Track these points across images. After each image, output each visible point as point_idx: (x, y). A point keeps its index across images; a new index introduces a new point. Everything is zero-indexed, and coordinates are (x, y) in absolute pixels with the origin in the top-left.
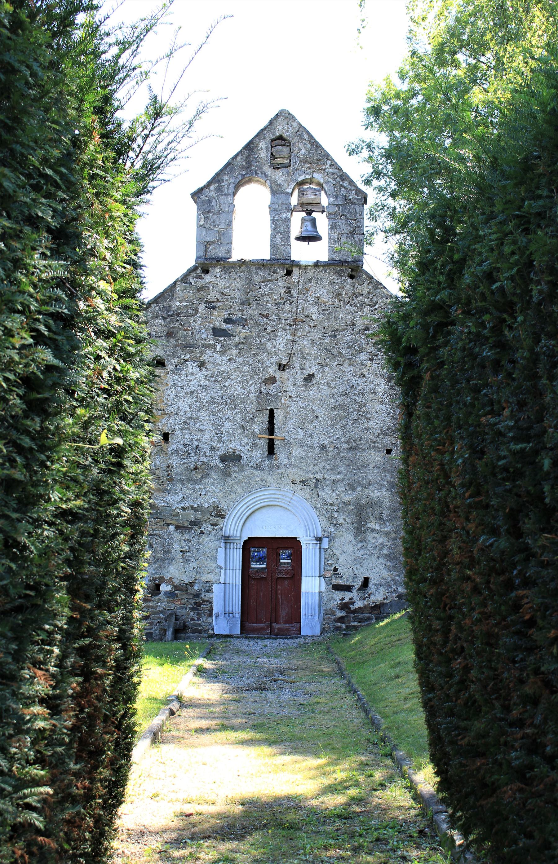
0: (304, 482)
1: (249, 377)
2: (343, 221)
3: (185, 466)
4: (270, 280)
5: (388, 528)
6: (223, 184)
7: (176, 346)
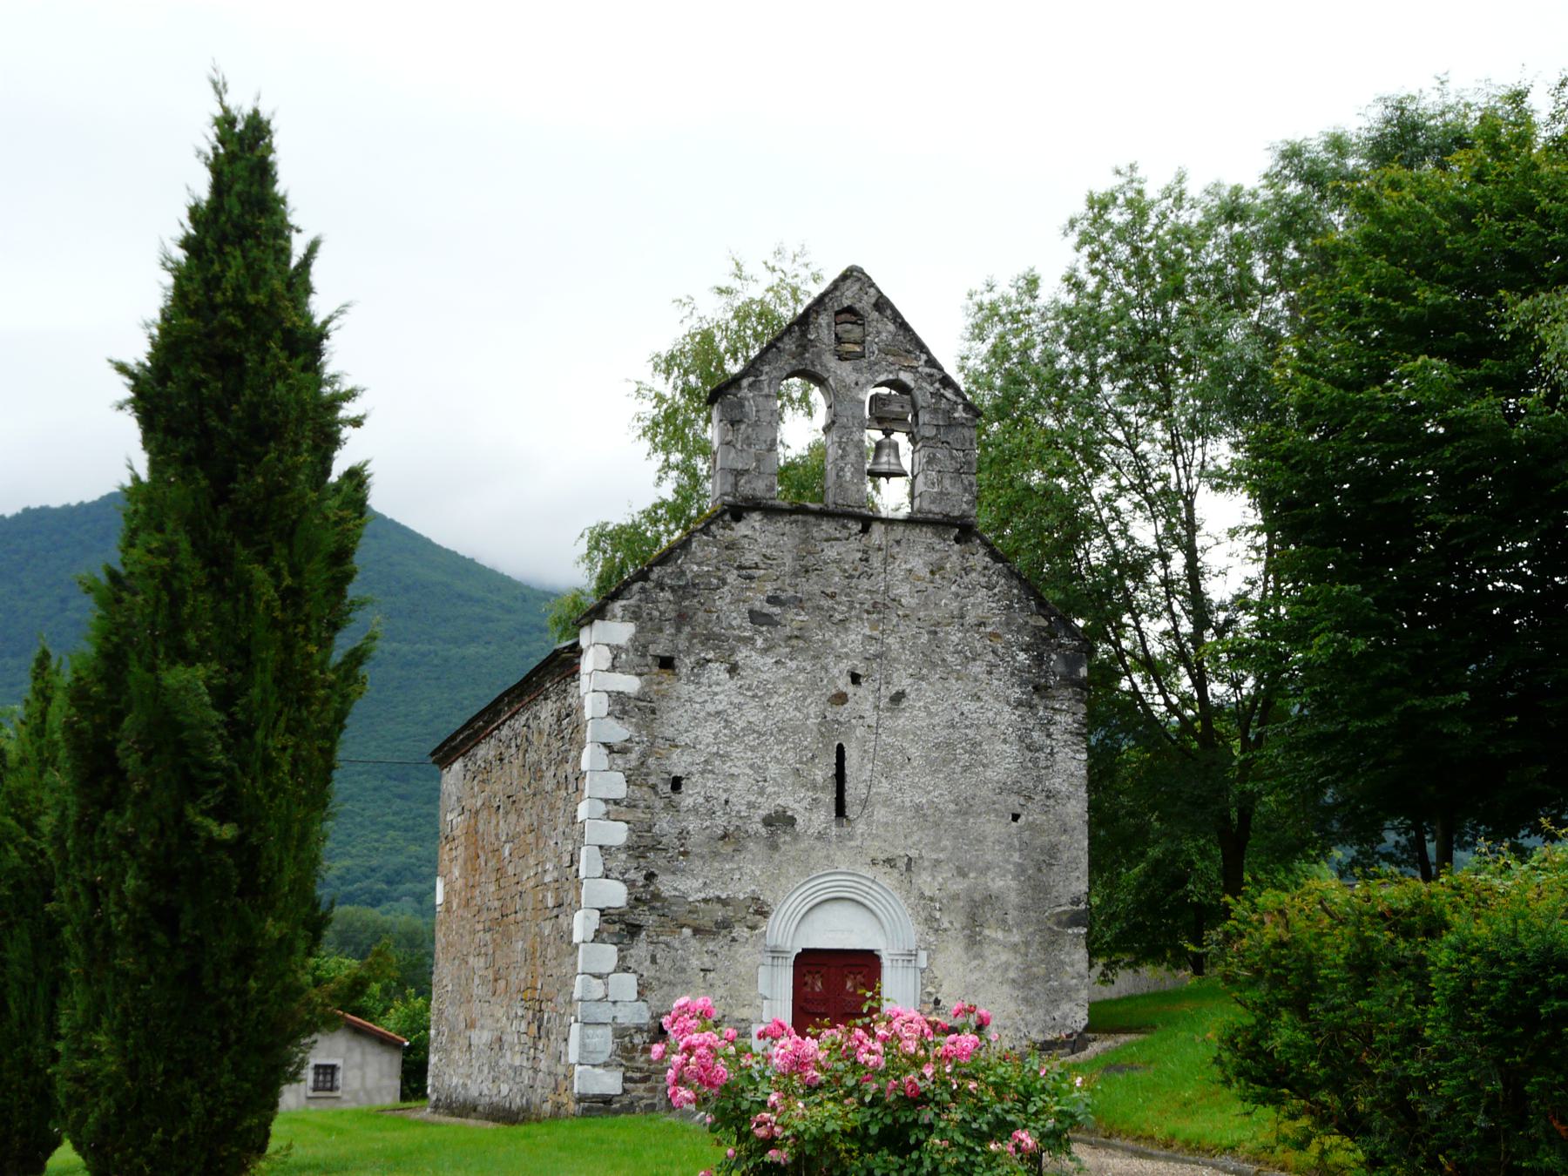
0: (890, 862)
1: (807, 693)
2: (946, 452)
3: (708, 831)
4: (837, 539)
5: (1016, 937)
6: (762, 378)
7: (694, 636)
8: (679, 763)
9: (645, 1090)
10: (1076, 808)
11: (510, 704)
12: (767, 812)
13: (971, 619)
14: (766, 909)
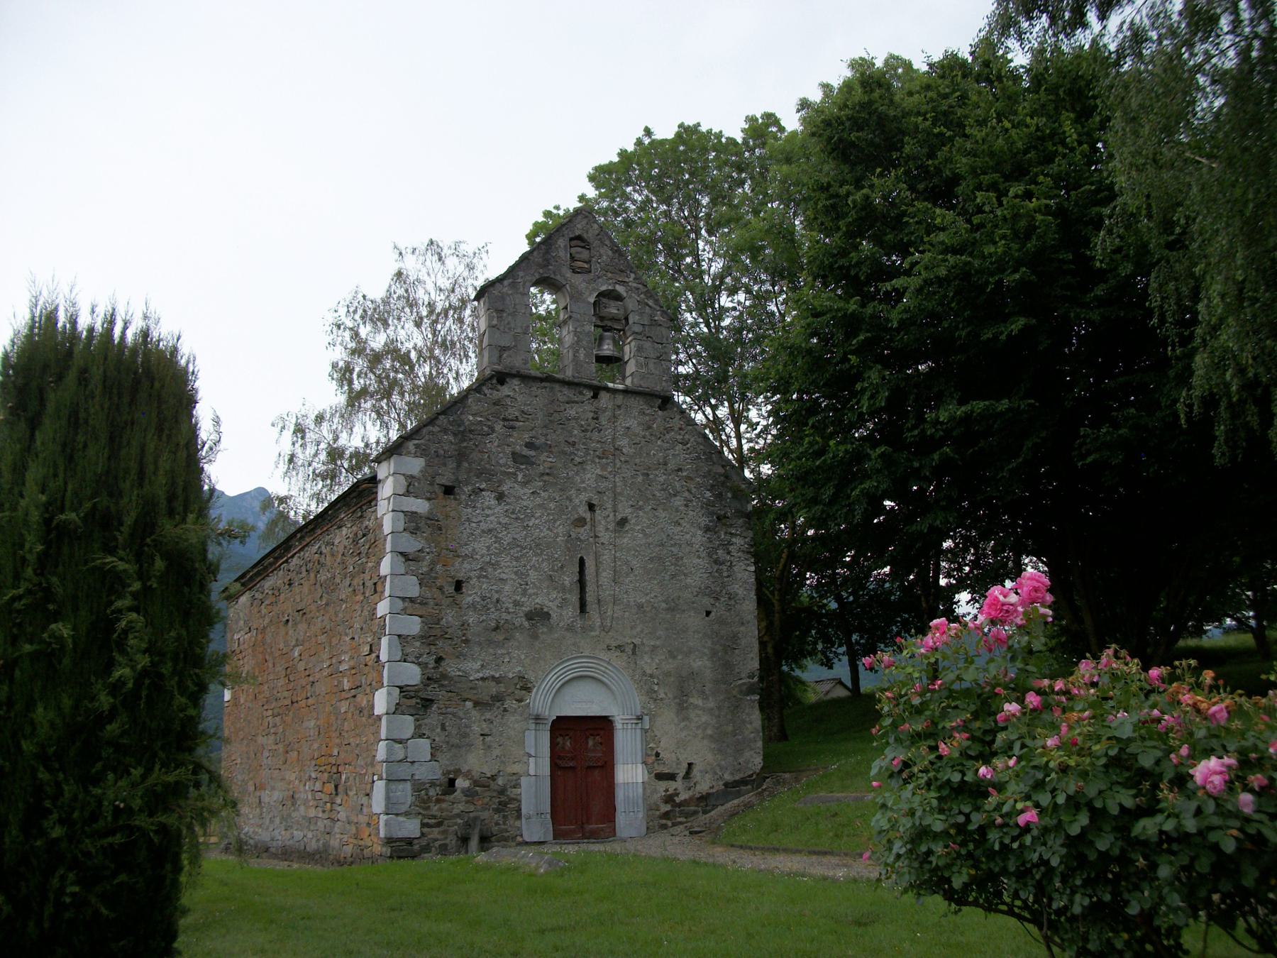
0: (619, 647)
3: (484, 624)
4: (577, 402)
5: (711, 704)
8: (462, 569)
9: (439, 833)
10: (749, 606)
11: (302, 538)
12: (528, 609)
13: (670, 466)
14: (529, 685)
